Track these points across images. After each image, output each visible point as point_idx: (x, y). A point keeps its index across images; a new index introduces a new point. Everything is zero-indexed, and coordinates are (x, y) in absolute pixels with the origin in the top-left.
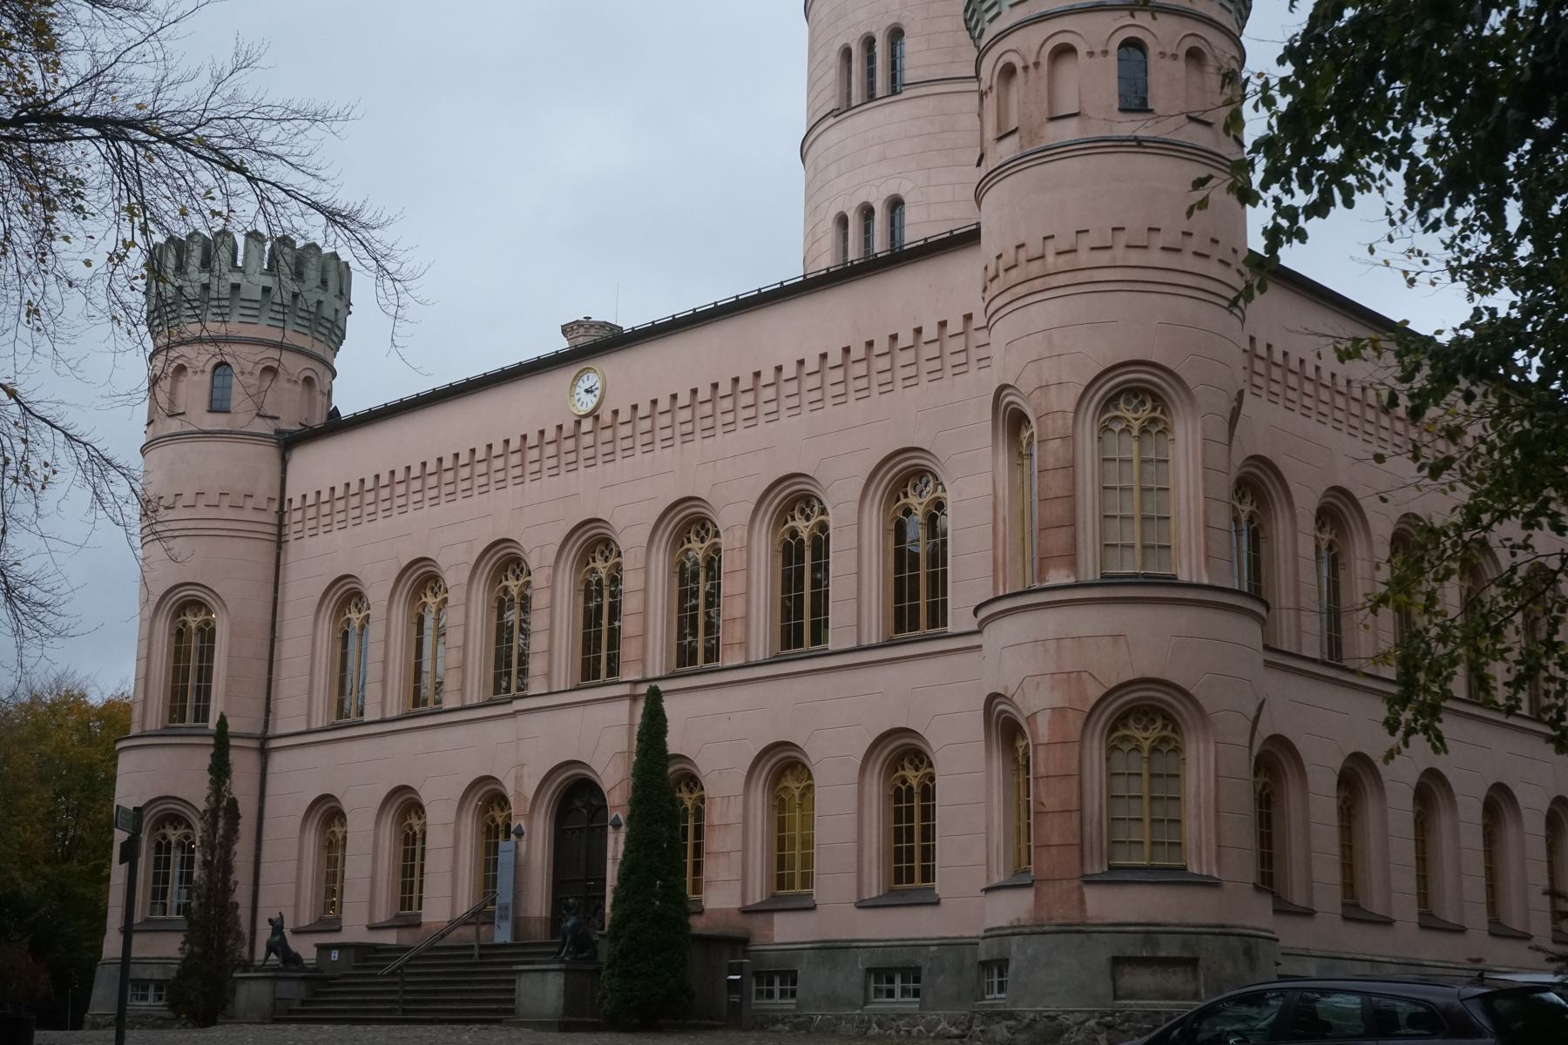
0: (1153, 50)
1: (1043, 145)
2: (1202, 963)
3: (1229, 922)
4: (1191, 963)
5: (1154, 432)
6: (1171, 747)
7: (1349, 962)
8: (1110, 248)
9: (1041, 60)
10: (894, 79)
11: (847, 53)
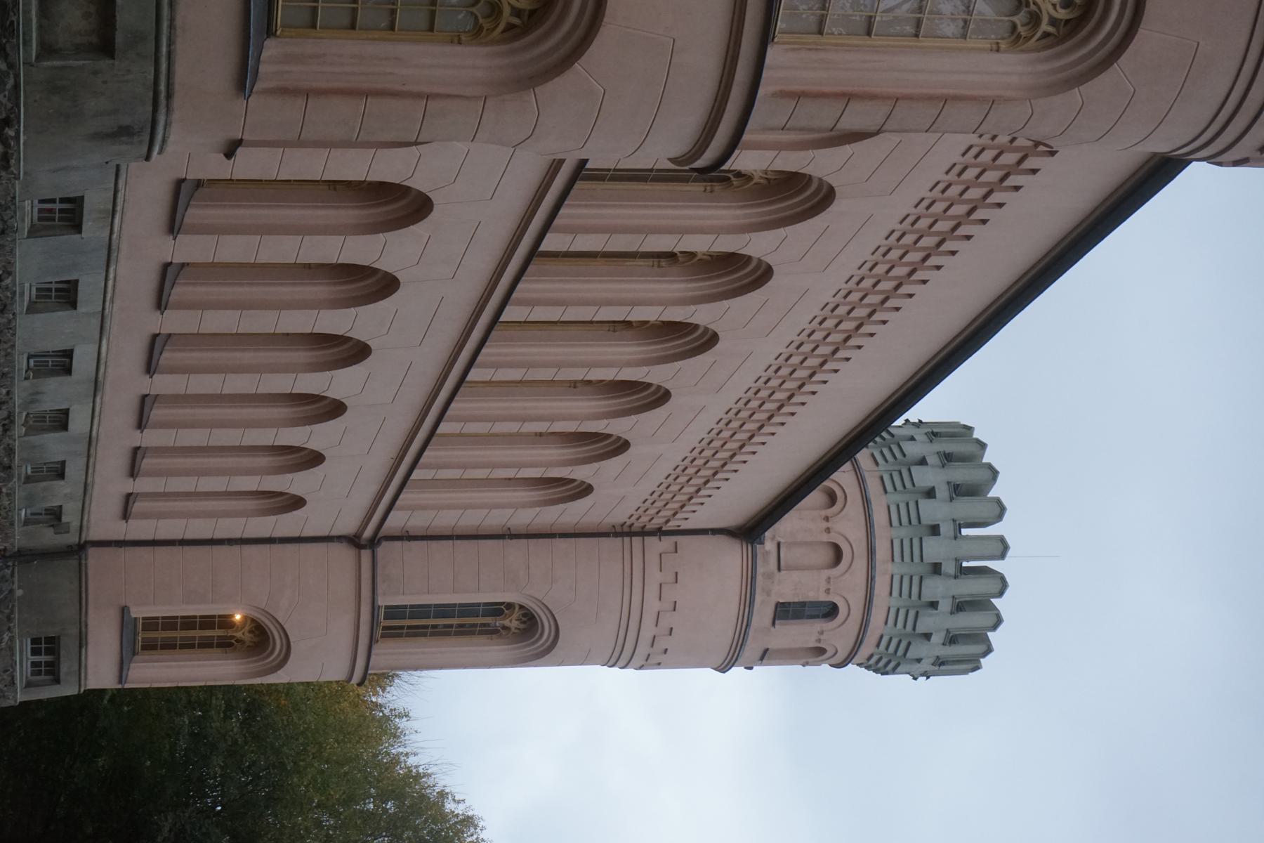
2: (104, 64)
3: (177, 102)
4: (105, 46)
5: (1016, 19)
6: (481, 21)
7: (112, 185)
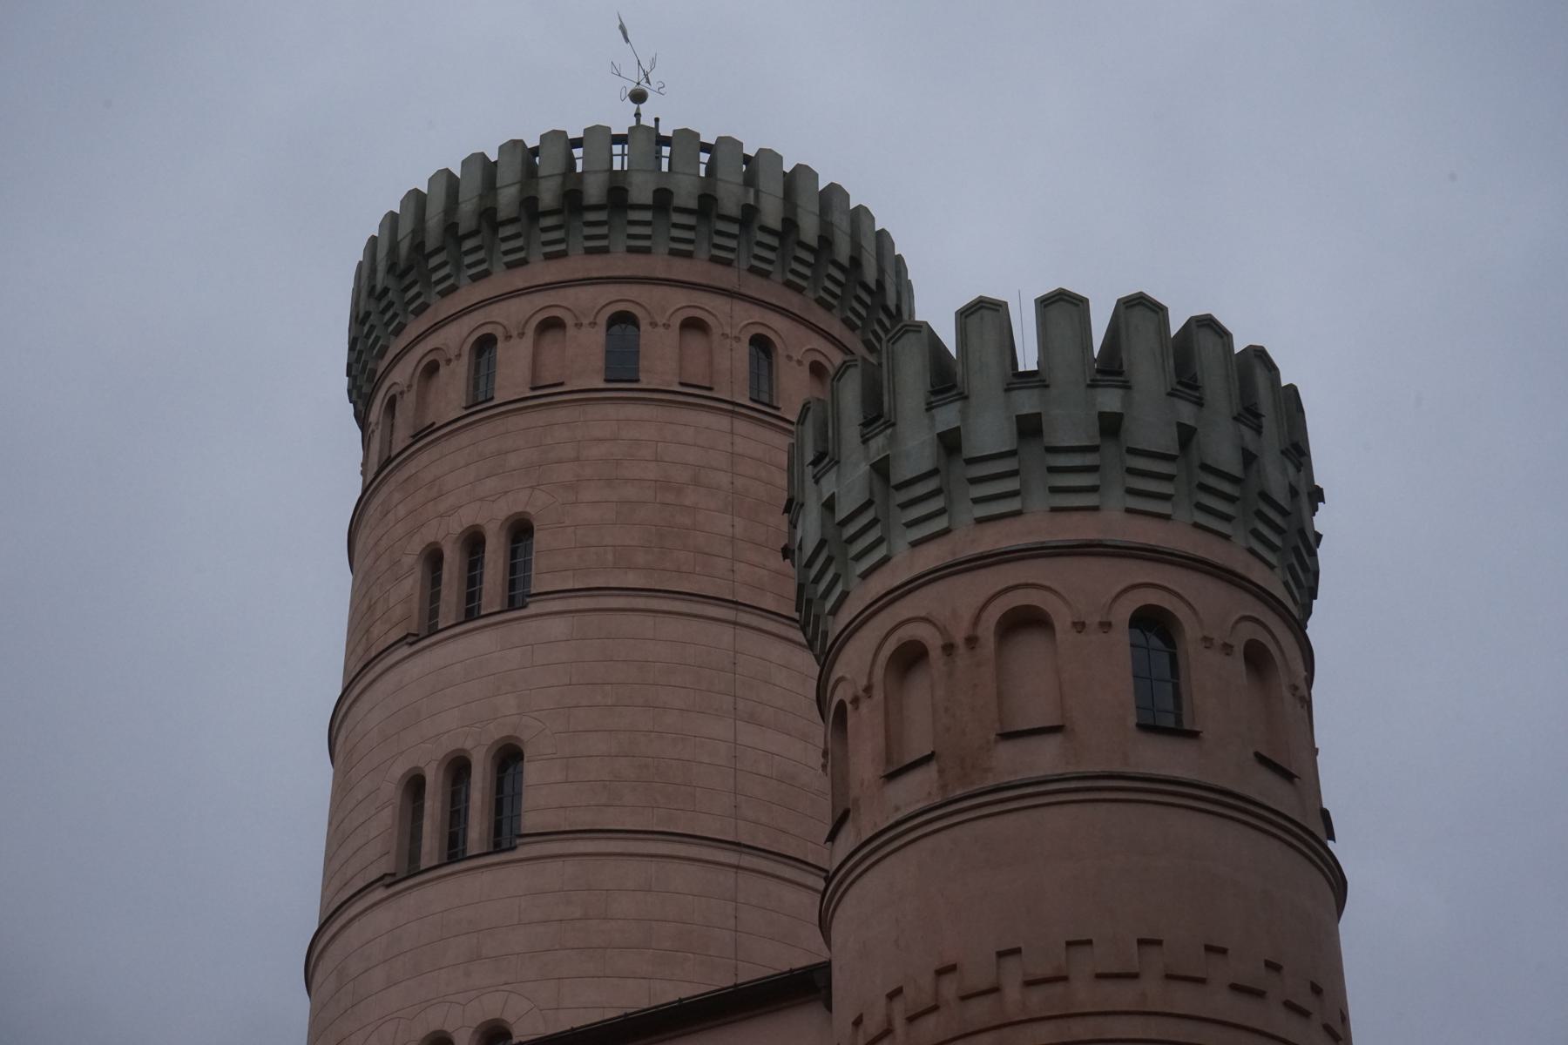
0: (1191, 632)
1: (990, 782)
8: (1134, 976)
9: (980, 632)
10: (498, 829)
11: (415, 785)
